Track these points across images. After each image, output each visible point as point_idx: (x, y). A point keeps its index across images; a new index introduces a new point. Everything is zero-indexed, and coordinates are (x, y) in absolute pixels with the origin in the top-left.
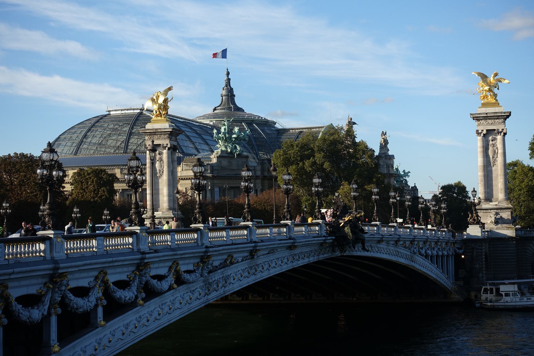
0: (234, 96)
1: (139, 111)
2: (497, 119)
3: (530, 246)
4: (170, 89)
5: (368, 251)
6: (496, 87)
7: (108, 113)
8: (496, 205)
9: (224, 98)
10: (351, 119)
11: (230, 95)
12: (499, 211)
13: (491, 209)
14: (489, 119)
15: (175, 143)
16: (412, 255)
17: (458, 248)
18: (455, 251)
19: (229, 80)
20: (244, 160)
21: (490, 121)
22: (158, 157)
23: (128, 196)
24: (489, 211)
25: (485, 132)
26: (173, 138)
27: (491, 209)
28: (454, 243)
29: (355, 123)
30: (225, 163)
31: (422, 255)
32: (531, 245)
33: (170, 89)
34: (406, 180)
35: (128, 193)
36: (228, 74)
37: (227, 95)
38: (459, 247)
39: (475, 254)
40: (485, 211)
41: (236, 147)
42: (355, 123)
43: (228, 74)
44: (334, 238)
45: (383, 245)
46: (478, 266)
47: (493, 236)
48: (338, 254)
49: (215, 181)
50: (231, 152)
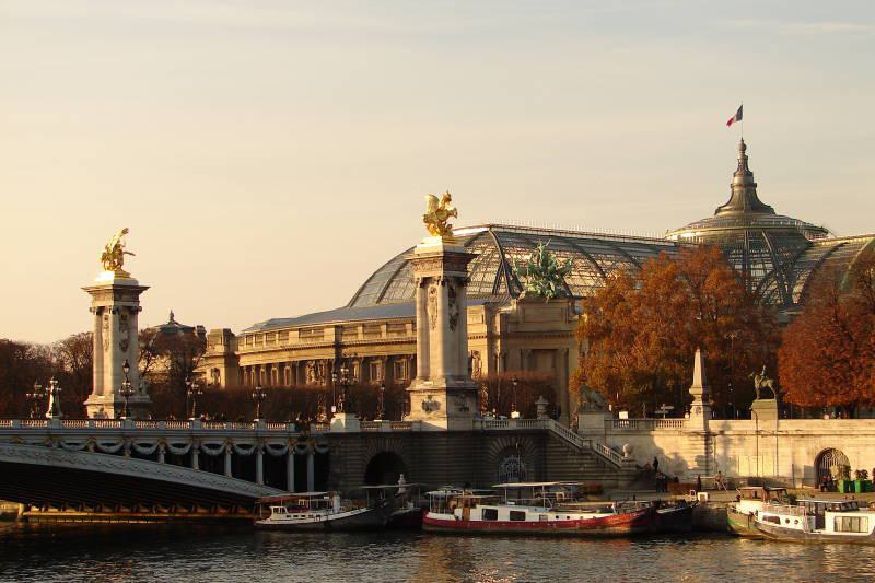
4: (125, 231)
9: (736, 190)
11: (748, 183)
13: (425, 391)
18: (315, 450)
22: (105, 322)
26: (124, 297)
27: (425, 391)
31: (120, 453)
32: (495, 443)
33: (125, 231)
36: (744, 147)
37: (739, 185)
41: (550, 287)
43: (744, 147)
46: (338, 471)
47: (424, 430)
49: (512, 341)
50: (543, 294)
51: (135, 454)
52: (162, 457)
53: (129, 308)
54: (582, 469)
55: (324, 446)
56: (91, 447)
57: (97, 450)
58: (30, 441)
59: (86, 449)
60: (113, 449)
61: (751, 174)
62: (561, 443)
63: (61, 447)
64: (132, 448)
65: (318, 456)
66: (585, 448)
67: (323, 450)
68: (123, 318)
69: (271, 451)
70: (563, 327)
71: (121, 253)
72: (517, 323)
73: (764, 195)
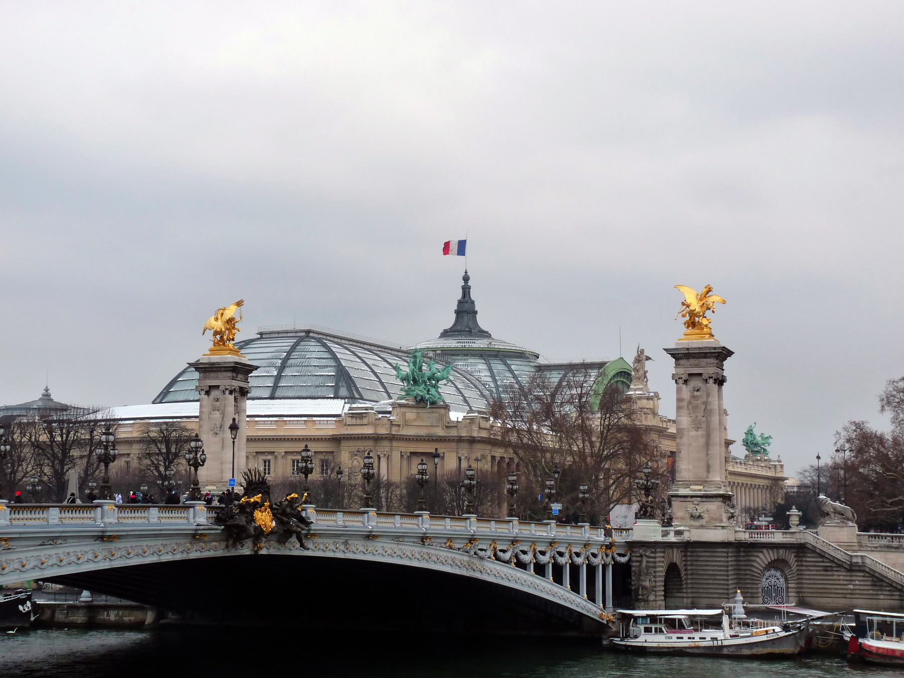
0: (456, 312)
1: (303, 334)
2: (705, 357)
3: (758, 556)
5: (308, 549)
6: (708, 309)
7: (259, 336)
8: (700, 490)
10: (642, 351)
12: (704, 499)
14: (694, 358)
15: (243, 384)
16: (476, 561)
17: (620, 555)
18: (613, 558)
19: (469, 288)
20: (443, 411)
21: (692, 361)
23: (265, 462)
24: (689, 499)
25: (685, 377)
26: (240, 376)
28: (609, 546)
29: (648, 358)
30: (411, 415)
31: (508, 562)
32: (761, 555)
34: (765, 450)
35: (265, 458)
36: (466, 279)
38: (622, 552)
39: (644, 564)
40: (682, 499)
42: (648, 358)
43: (466, 279)
45: (378, 545)
46: (647, 584)
48: (246, 550)
49: (395, 444)
51: (521, 565)
52: (532, 565)
53: (241, 389)
54: (851, 587)
55: (624, 556)
56: (492, 556)
57: (498, 558)
58: (457, 546)
59: (489, 558)
60: (507, 556)
61: (473, 302)
62: (822, 557)
63: (475, 554)
64: (516, 556)
65: (617, 566)
66: (856, 564)
67: (623, 560)
68: (235, 399)
69: (592, 559)
70: (440, 432)
71: (234, 328)
72: (399, 426)
73: (483, 321)
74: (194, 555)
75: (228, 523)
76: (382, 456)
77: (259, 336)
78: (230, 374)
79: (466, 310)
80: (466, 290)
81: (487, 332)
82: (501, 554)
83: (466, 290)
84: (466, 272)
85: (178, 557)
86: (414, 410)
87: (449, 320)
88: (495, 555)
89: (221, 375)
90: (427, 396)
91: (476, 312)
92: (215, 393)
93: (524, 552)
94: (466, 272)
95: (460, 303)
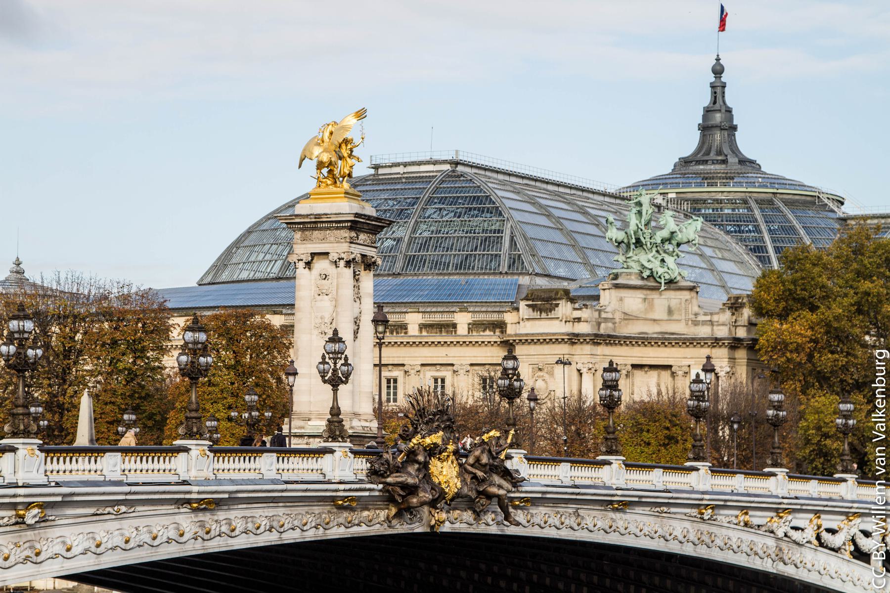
36: (718, 71)
43: (718, 71)
44: (381, 486)
51: (861, 555)
61: (729, 111)
73: (748, 143)
74: (337, 532)
75: (389, 480)
76: (584, 371)
77: (372, 171)
78: (346, 234)
79: (718, 123)
80: (718, 89)
81: (752, 162)
82: (825, 536)
83: (718, 89)
84: (718, 60)
85: (311, 535)
86: (640, 294)
87: (688, 142)
88: (818, 538)
89: (331, 235)
90: (661, 271)
91: (734, 128)
92: (321, 265)
93: (867, 534)
94: (718, 60)
95: (708, 111)
